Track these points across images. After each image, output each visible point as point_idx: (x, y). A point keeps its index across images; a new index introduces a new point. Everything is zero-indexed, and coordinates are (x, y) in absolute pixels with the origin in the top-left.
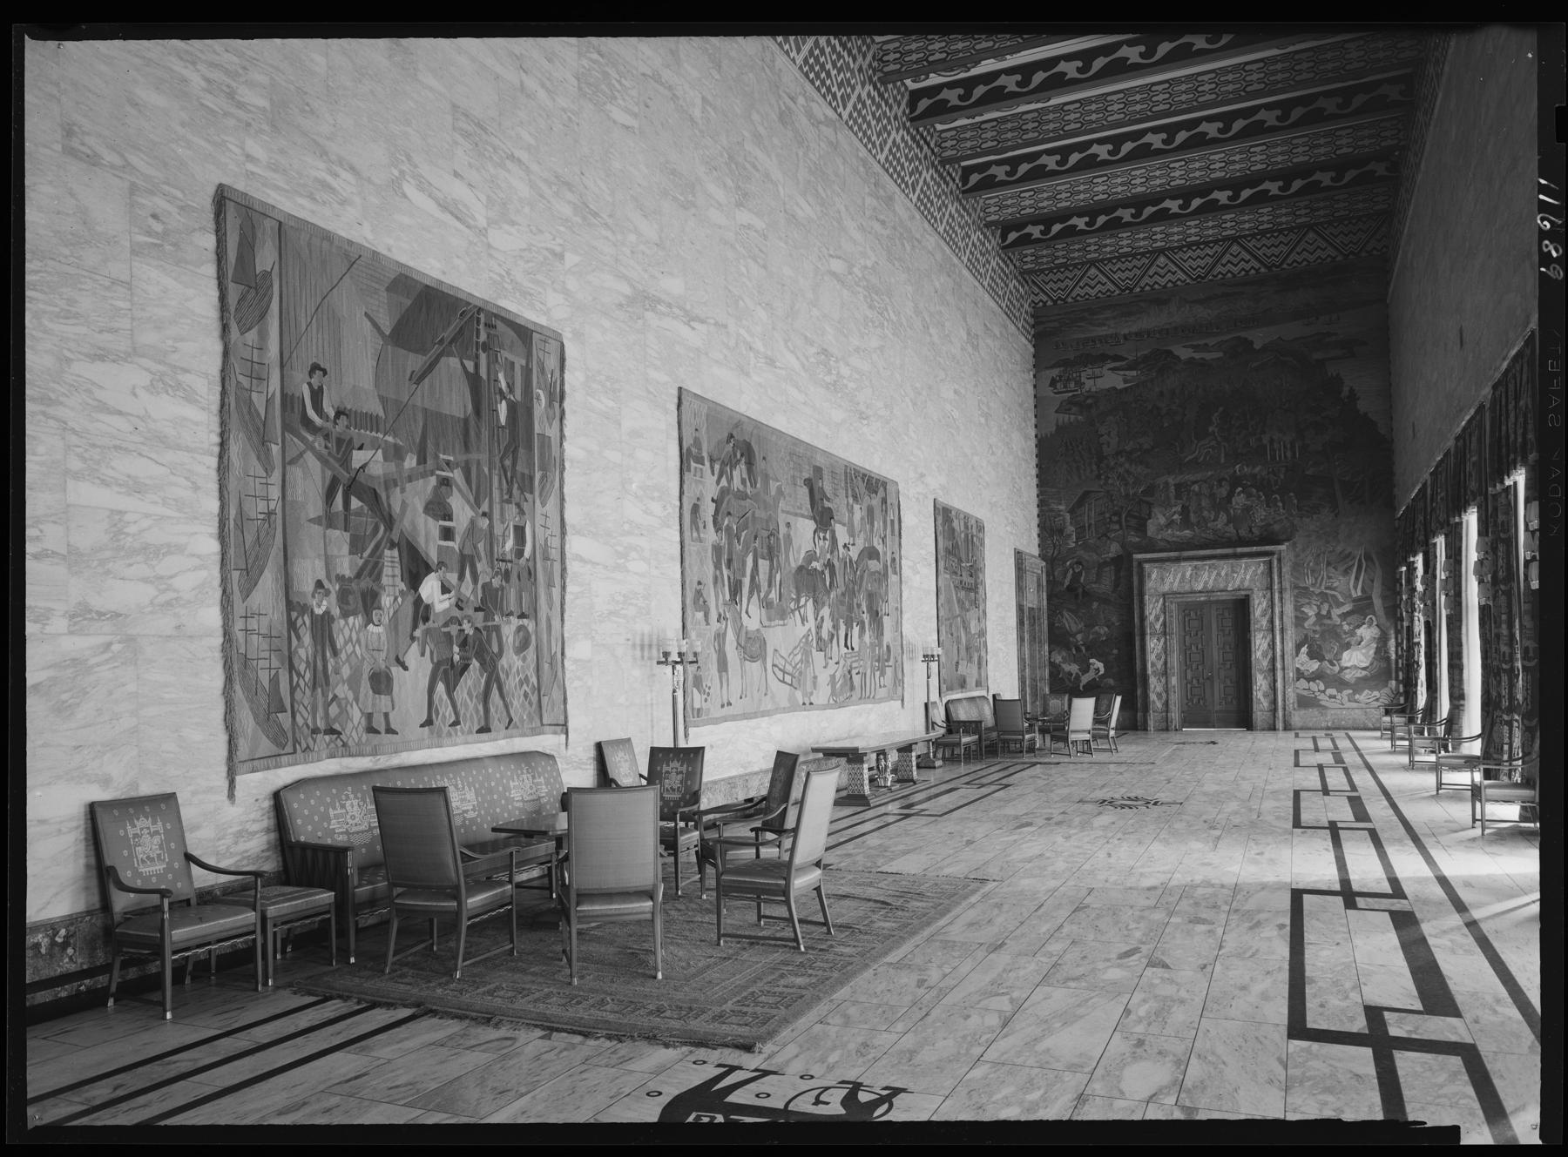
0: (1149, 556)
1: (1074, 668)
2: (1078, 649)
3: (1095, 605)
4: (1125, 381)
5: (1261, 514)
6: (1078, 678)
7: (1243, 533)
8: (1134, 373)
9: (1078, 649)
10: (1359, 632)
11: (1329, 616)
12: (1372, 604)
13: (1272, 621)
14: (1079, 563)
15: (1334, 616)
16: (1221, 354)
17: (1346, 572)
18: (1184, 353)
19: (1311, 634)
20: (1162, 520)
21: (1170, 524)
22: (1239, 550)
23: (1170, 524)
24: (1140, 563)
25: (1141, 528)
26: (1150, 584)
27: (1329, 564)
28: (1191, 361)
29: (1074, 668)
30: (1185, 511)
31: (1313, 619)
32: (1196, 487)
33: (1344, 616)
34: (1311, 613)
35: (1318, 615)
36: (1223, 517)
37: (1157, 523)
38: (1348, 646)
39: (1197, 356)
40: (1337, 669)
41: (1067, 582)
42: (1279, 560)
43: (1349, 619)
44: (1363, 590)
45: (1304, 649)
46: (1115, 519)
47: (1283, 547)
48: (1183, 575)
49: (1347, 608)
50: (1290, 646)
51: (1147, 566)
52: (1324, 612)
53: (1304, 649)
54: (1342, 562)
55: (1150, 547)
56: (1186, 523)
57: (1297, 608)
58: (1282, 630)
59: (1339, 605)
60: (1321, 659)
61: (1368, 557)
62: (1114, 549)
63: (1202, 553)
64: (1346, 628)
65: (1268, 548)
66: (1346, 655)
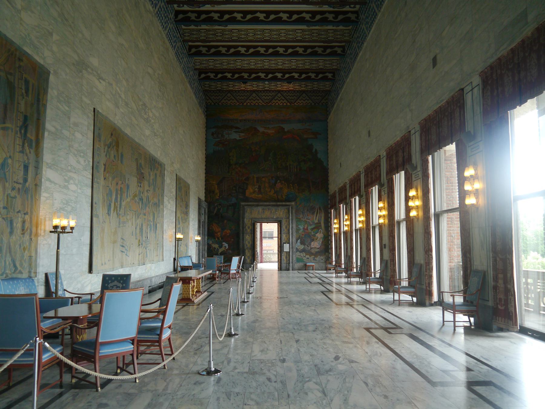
0: (247, 203)
1: (216, 246)
2: (218, 238)
3: (225, 221)
4: (240, 137)
5: (286, 191)
6: (218, 250)
7: (279, 197)
8: (243, 134)
9: (218, 238)
10: (317, 235)
11: (307, 229)
12: (321, 226)
13: (289, 230)
14: (220, 205)
15: (309, 230)
16: (274, 132)
17: (313, 213)
18: (261, 129)
19: (301, 235)
20: (252, 191)
21: (254, 192)
22: (278, 203)
23: (254, 192)
24: (243, 206)
25: (244, 193)
26: (247, 215)
27: (307, 210)
28: (263, 133)
29: (216, 246)
30: (259, 188)
31: (302, 230)
32: (264, 179)
33: (312, 229)
34: (301, 228)
35: (304, 228)
36: (273, 191)
37: (250, 191)
38: (313, 240)
39: (266, 131)
40: (309, 248)
41: (215, 212)
42: (292, 208)
43: (314, 230)
44: (318, 221)
45: (299, 241)
46: (234, 188)
47: (293, 203)
48: (259, 211)
49: (313, 227)
50: (294, 239)
51: (246, 207)
52: (306, 228)
53: (299, 241)
54: (312, 210)
55: (247, 200)
56: (260, 192)
57: (297, 226)
58: (292, 233)
59: (311, 225)
60: (304, 245)
61: (320, 209)
62: (234, 200)
63: (265, 203)
64: (313, 233)
65: (288, 203)
66: (312, 243)
